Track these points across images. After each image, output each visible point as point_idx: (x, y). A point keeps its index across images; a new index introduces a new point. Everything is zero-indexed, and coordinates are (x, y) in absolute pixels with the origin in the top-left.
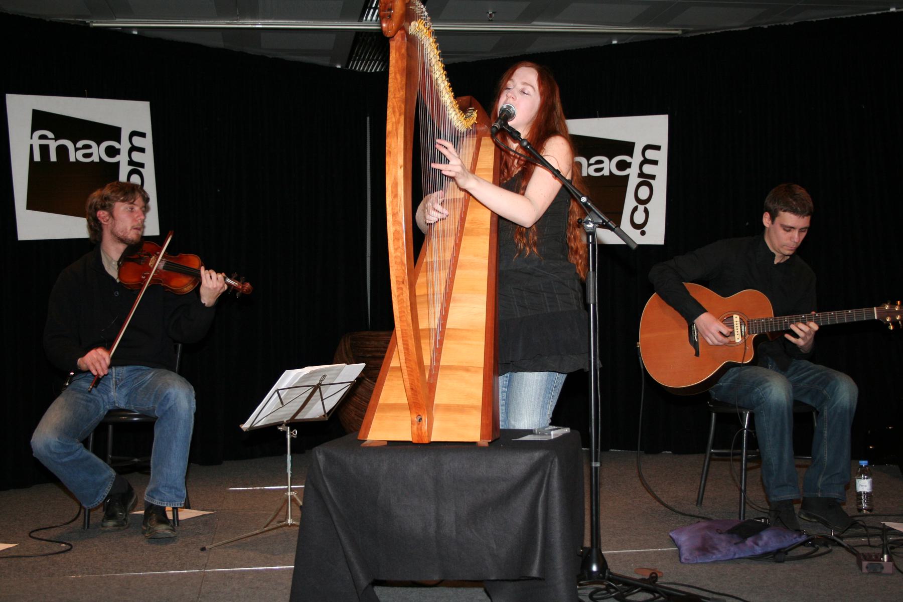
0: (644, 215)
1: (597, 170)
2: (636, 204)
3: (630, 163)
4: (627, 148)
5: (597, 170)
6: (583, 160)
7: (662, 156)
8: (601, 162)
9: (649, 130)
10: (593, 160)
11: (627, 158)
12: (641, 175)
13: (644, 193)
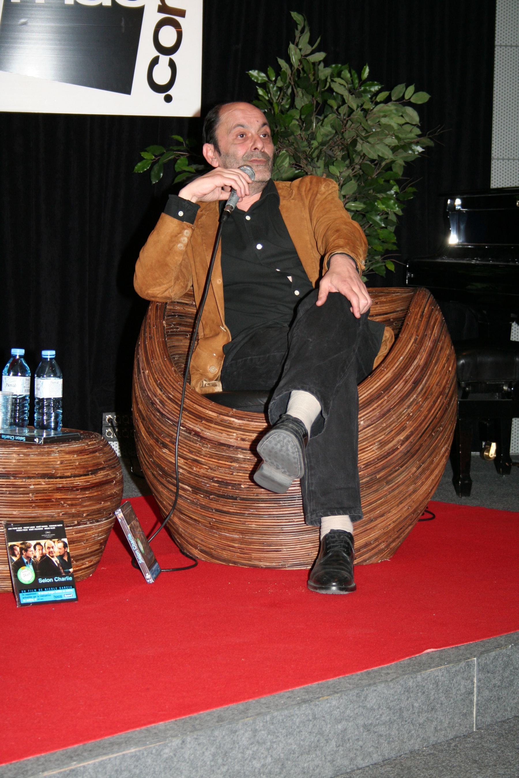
0: (168, 72)
2: (157, 54)
13: (168, 36)
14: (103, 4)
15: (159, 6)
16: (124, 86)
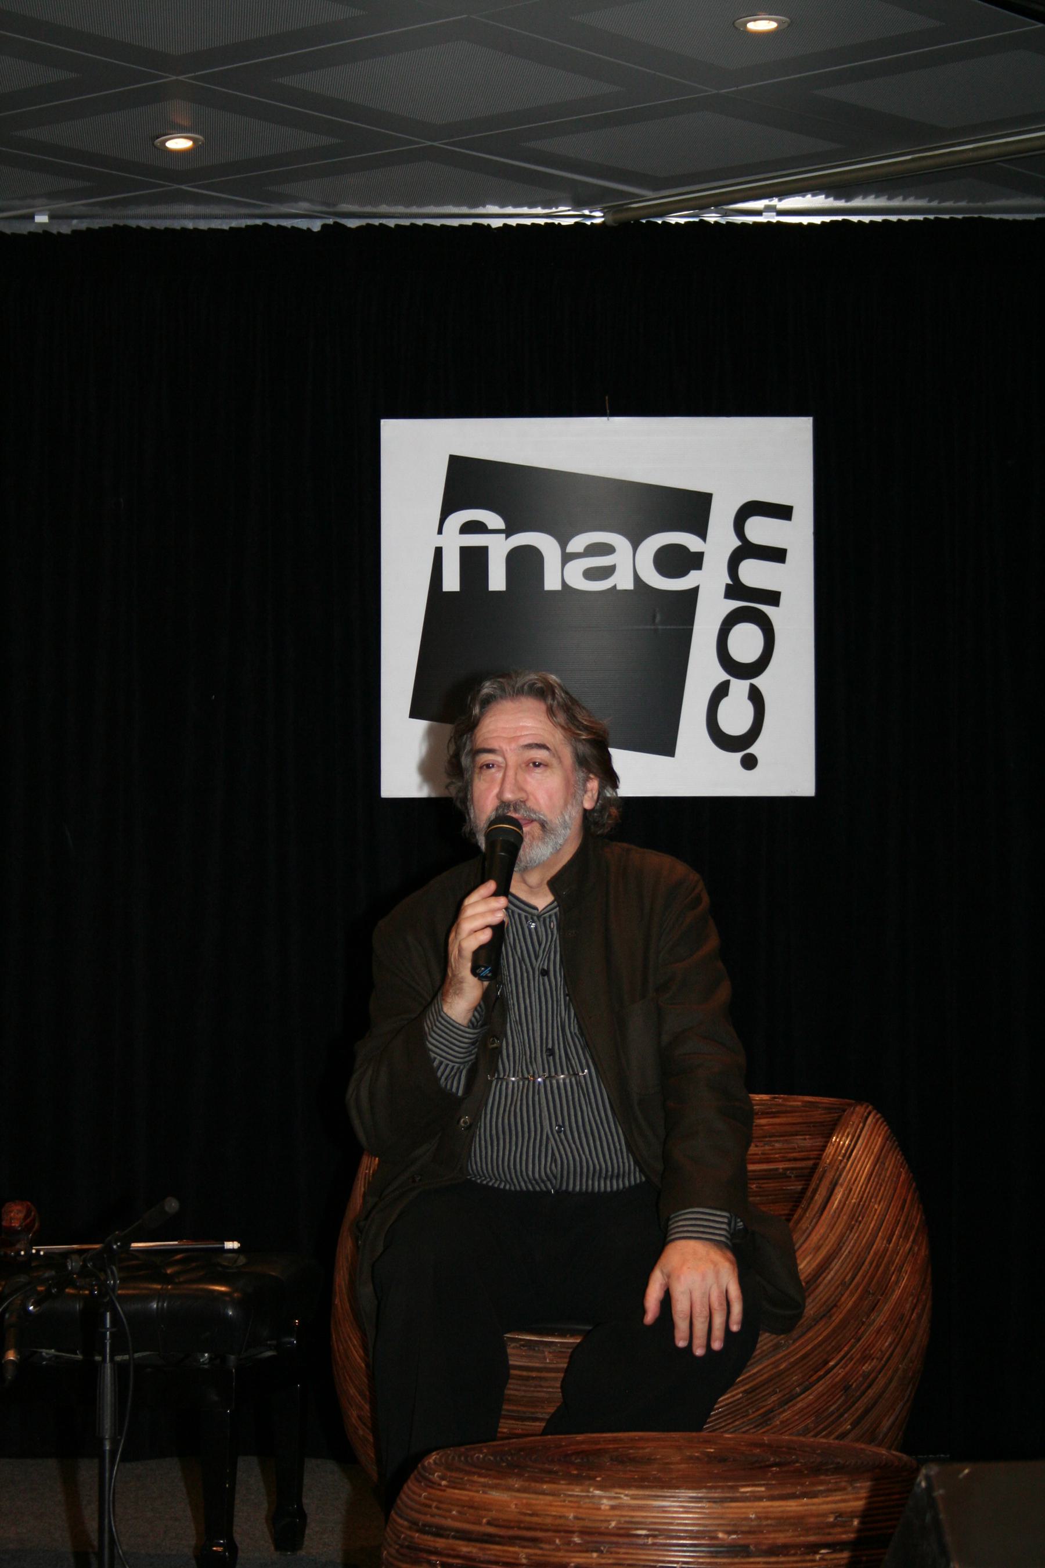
0: (749, 709)
1: (591, 574)
2: (724, 676)
3: (700, 556)
4: (691, 509)
5: (591, 574)
6: (545, 543)
7: (798, 536)
8: (607, 549)
9: (757, 461)
10: (578, 543)
11: (690, 541)
12: (735, 589)
13: (745, 643)
14: (619, 588)
15: (728, 585)
16: (663, 742)
